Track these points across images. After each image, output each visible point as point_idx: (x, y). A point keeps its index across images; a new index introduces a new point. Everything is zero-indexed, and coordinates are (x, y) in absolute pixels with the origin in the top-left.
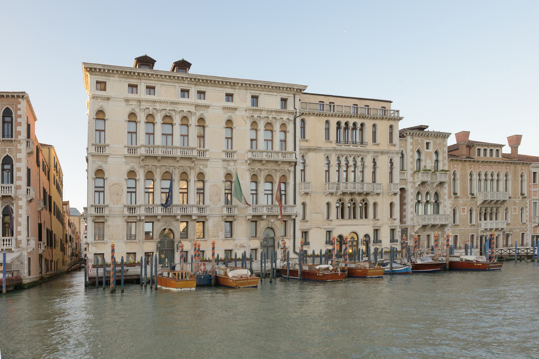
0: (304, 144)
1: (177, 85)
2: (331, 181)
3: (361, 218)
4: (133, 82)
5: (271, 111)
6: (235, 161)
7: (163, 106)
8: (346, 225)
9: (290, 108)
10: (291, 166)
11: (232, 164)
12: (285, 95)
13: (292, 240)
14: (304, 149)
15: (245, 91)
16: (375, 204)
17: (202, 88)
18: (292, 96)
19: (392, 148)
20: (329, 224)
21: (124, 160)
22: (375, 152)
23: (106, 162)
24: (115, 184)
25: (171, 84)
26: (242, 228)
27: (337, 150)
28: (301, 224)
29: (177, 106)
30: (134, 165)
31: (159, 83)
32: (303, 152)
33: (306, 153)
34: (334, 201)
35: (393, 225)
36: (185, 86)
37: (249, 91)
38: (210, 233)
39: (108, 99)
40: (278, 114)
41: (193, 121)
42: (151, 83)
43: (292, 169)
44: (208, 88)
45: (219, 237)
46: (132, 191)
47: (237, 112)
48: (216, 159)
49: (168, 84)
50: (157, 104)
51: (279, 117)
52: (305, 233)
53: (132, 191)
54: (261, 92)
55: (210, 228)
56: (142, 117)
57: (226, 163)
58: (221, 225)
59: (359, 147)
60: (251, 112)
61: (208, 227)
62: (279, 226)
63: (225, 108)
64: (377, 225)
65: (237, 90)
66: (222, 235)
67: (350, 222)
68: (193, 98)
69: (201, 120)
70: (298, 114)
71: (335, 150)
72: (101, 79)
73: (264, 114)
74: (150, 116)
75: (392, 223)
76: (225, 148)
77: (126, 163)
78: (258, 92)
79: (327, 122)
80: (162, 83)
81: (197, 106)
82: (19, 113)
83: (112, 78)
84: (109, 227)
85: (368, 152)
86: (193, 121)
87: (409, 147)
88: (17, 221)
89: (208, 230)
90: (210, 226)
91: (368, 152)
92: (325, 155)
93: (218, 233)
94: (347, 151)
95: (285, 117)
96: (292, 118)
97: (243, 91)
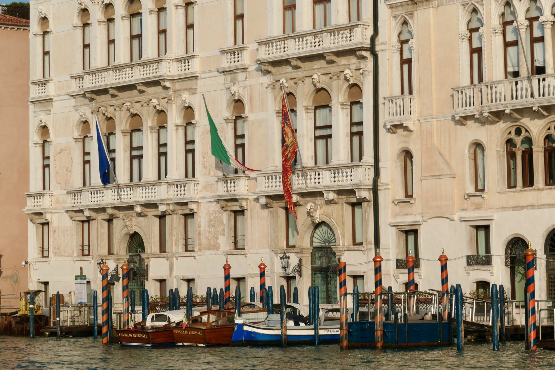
2: (486, 79)
8: (533, 207)
11: (241, 76)
20: (478, 207)
21: (73, 101)
23: (49, 112)
24: (62, 150)
28: (398, 209)
30: (86, 111)
32: (401, 12)
33: (411, 14)
34: (494, 136)
38: (203, 240)
45: (218, 248)
48: (210, 71)
52: (410, 232)
55: (202, 229)
57: (229, 77)
58: (222, 221)
61: (199, 226)
62: (339, 215)
84: (54, 232)
93: (217, 238)
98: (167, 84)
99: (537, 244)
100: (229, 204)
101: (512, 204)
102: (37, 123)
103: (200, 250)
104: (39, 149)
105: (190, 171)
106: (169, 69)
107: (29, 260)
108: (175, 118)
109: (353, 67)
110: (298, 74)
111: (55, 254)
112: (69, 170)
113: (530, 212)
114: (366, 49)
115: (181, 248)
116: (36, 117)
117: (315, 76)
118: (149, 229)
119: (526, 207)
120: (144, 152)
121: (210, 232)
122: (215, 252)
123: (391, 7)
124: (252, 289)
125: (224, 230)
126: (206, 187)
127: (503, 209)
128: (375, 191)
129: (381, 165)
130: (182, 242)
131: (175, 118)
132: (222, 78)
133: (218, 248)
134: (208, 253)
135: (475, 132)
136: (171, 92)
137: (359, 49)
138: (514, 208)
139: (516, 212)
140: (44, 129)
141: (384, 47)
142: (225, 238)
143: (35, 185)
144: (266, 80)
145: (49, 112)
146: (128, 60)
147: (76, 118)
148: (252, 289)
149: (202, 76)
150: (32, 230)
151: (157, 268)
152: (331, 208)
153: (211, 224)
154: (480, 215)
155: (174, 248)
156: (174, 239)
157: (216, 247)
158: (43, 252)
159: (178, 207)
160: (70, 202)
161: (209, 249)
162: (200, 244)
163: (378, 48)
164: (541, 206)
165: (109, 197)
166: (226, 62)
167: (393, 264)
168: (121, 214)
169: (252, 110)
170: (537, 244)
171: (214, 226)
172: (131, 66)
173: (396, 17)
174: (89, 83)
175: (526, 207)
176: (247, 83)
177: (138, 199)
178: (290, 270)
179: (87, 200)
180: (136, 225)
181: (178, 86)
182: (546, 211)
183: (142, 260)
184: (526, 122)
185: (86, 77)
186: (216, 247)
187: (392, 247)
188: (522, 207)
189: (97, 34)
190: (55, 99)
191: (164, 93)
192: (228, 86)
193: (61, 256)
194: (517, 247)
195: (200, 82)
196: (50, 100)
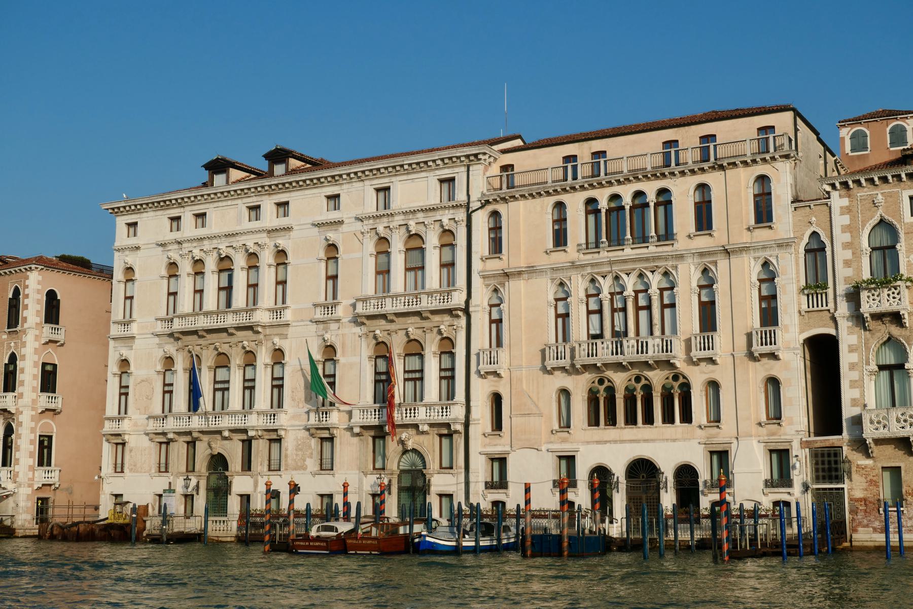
0: (495, 265)
1: (239, 202)
3: (668, 418)
4: (174, 212)
5: (414, 212)
6: (338, 320)
7: (215, 243)
8: (615, 442)
9: (461, 197)
10: (458, 316)
11: (333, 326)
12: (447, 171)
13: (462, 478)
14: (494, 276)
15: (361, 184)
16: (714, 385)
17: (282, 198)
18: (464, 169)
19: (763, 235)
20: (564, 441)
21: (157, 340)
22: (702, 254)
23: (131, 348)
24: (143, 381)
25: (229, 203)
26: (351, 452)
27: (583, 266)
28: (487, 440)
29: (238, 238)
30: (171, 348)
31: (212, 205)
33: (503, 285)
34: (579, 386)
35: (775, 438)
36: (253, 201)
37: (367, 183)
38: (290, 461)
39: (138, 248)
40: (430, 214)
41: (267, 258)
42: (199, 209)
43: (463, 322)
44: (293, 194)
45: (305, 469)
46: (168, 391)
47: (344, 228)
48: (302, 321)
49: (224, 203)
50: (206, 242)
51: (431, 220)
53: (168, 391)
54: (393, 179)
55: (289, 452)
56: (186, 267)
57: (321, 326)
58: (310, 446)
59: (652, 249)
60: (371, 221)
61: (286, 450)
62: (429, 445)
63: (318, 225)
64: (715, 440)
65: (345, 187)
66: (312, 464)
67: (630, 432)
68: (269, 217)
69: (281, 252)
70: (475, 205)
71: (574, 266)
72: (131, 218)
73: (399, 220)
74: (198, 262)
75: (773, 434)
76: (322, 299)
77: (160, 345)
78: (387, 180)
79: (560, 206)
80: (216, 205)
81: (271, 232)
82: (27, 291)
83: (145, 215)
84: (131, 451)
85: (681, 257)
86: (267, 258)
87: (840, 221)
88: (16, 444)
89: (286, 456)
90: (290, 448)
91: (681, 257)
92: (553, 280)
93: (304, 460)
94: (611, 263)
95: (445, 217)
96: (461, 215)
97: (358, 185)
98: (260, 329)
99: (619, 471)
100: (319, 432)
101: (596, 438)
102: (117, 356)
103: (286, 469)
104: (117, 379)
105: (279, 403)
106: (261, 317)
107: (102, 475)
108: (264, 357)
109: (448, 323)
110: (392, 327)
111: (131, 470)
112: (149, 398)
113: (613, 446)
114: (461, 310)
115: (266, 468)
116: (115, 352)
117: (410, 329)
118: (233, 452)
119: (609, 442)
120: (174, 388)
121: (297, 455)
122: (302, 472)
123: (484, 277)
124: (460, 504)
125: (312, 454)
126: (294, 417)
127: (588, 443)
128: (467, 425)
129: (472, 404)
130: (266, 463)
131: (264, 357)
132: (314, 327)
133: (305, 469)
134: (294, 472)
135: (561, 380)
136: (261, 336)
137: (456, 309)
138: (598, 442)
139: (600, 446)
140: (124, 363)
141: (477, 309)
142: (312, 460)
143: (111, 409)
144: (358, 330)
145: (131, 348)
146: (191, 311)
147: (160, 354)
148: (460, 504)
149: (294, 324)
150: (107, 449)
151: (240, 484)
152: (422, 438)
153: (298, 448)
154: (566, 448)
155: (259, 468)
156: (260, 460)
157: (304, 468)
158: (116, 468)
159: (265, 433)
160: (153, 426)
161: (295, 469)
162: (286, 465)
163: (471, 309)
164: (622, 441)
165: (197, 423)
166: (319, 314)
167: (482, 486)
168: (205, 438)
169: (343, 354)
170: (619, 471)
171: (301, 450)
172: (194, 314)
173: (487, 286)
174: (177, 325)
175: (609, 442)
176: (340, 332)
177: (226, 425)
178: (190, 489)
179: (171, 425)
180: (219, 447)
181: (268, 331)
182: (628, 445)
183: (227, 477)
184: (610, 374)
185: (176, 320)
186: (304, 468)
187: (481, 470)
188: (606, 442)
189: (186, 286)
190: (137, 337)
191: (254, 337)
192: (320, 333)
193: (137, 472)
194: (601, 474)
195: (290, 329)
196: (133, 338)
